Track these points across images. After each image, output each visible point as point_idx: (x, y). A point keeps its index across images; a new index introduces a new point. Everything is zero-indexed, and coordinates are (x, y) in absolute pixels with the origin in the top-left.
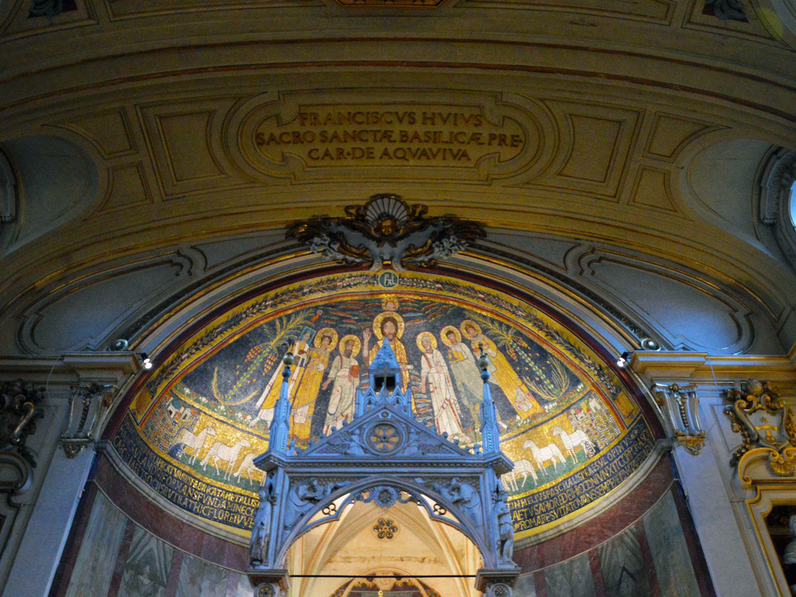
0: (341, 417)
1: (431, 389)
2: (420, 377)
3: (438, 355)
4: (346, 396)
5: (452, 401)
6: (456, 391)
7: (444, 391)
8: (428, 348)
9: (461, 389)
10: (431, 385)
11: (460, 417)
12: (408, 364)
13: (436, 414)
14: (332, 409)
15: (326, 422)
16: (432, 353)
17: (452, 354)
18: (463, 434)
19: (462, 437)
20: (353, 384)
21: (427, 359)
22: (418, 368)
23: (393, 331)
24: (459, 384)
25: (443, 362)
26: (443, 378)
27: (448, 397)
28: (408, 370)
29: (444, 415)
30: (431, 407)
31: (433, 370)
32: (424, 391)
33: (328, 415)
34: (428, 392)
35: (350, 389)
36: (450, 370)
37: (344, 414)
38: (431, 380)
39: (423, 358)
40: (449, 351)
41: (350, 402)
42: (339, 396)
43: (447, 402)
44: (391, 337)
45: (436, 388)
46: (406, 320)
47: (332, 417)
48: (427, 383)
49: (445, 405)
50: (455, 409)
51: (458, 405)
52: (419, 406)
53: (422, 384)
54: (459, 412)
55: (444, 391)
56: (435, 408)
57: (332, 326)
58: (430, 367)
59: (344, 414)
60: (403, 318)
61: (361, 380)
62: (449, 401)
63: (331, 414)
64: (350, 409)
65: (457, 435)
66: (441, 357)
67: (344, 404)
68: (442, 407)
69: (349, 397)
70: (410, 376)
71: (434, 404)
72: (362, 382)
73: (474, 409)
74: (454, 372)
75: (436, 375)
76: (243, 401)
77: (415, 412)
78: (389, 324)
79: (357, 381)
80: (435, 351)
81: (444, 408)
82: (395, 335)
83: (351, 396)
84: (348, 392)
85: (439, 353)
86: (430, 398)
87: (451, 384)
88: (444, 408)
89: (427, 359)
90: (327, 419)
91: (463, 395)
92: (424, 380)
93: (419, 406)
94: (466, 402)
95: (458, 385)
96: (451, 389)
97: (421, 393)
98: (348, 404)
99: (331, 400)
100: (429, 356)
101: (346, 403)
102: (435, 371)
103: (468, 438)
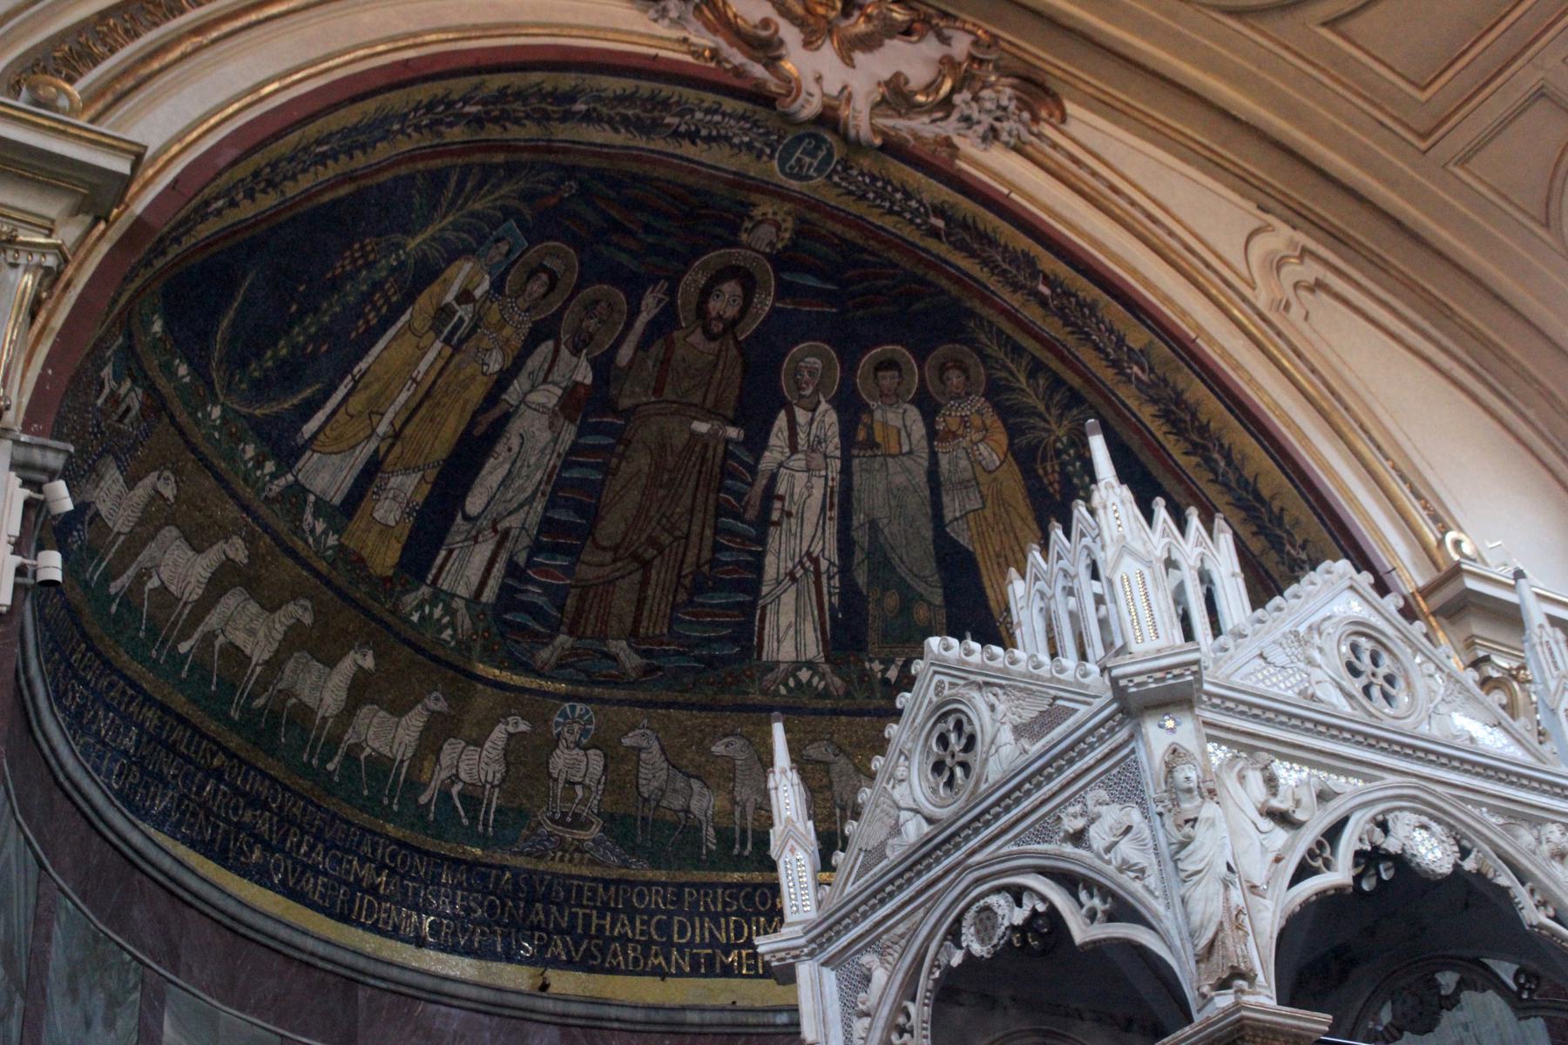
0: (488, 533)
1: (775, 516)
2: (753, 470)
3: (829, 418)
4: (524, 472)
5: (824, 565)
6: (846, 544)
7: (808, 530)
8: (808, 392)
9: (861, 536)
10: (777, 505)
11: (833, 618)
12: (734, 423)
13: (765, 590)
14: (475, 503)
15: (449, 540)
16: (814, 410)
17: (870, 428)
18: (827, 668)
19: (823, 677)
20: (555, 441)
21: (792, 424)
22: (757, 442)
24: (859, 519)
25: (833, 445)
26: (818, 493)
27: (816, 551)
28: (728, 441)
29: (789, 598)
30: (759, 568)
31: (798, 461)
32: (751, 514)
33: (459, 517)
34: (764, 522)
35: (543, 451)
36: (846, 471)
37: (501, 526)
38: (782, 489)
39: (782, 415)
40: (865, 418)
41: (527, 494)
42: (507, 466)
43: (808, 564)
45: (789, 515)
47: (467, 526)
48: (770, 495)
49: (799, 573)
50: (825, 590)
51: (836, 582)
52: (725, 557)
54: (835, 600)
55: (808, 530)
56: (770, 572)
58: (794, 448)
59: (501, 526)
61: (579, 435)
62: (815, 561)
63: (466, 518)
64: (522, 514)
65: (810, 665)
66: (836, 429)
67: (510, 495)
68: (792, 576)
69: (533, 478)
70: (725, 459)
71: (770, 560)
72: (582, 441)
73: (879, 602)
74: (856, 480)
75: (801, 478)
77: (706, 569)
79: (569, 434)
80: (824, 406)
81: (794, 579)
83: (538, 476)
84: (533, 460)
85: (832, 417)
86: (762, 540)
87: (835, 513)
88: (794, 579)
89: (792, 424)
90: (454, 529)
91: (859, 556)
92: (762, 482)
93: (725, 557)
94: (861, 579)
95: (855, 523)
96: (832, 529)
97: (738, 517)
98: (522, 497)
99: (484, 472)
100: (802, 416)
101: (514, 496)
102: (803, 464)
103: (838, 681)
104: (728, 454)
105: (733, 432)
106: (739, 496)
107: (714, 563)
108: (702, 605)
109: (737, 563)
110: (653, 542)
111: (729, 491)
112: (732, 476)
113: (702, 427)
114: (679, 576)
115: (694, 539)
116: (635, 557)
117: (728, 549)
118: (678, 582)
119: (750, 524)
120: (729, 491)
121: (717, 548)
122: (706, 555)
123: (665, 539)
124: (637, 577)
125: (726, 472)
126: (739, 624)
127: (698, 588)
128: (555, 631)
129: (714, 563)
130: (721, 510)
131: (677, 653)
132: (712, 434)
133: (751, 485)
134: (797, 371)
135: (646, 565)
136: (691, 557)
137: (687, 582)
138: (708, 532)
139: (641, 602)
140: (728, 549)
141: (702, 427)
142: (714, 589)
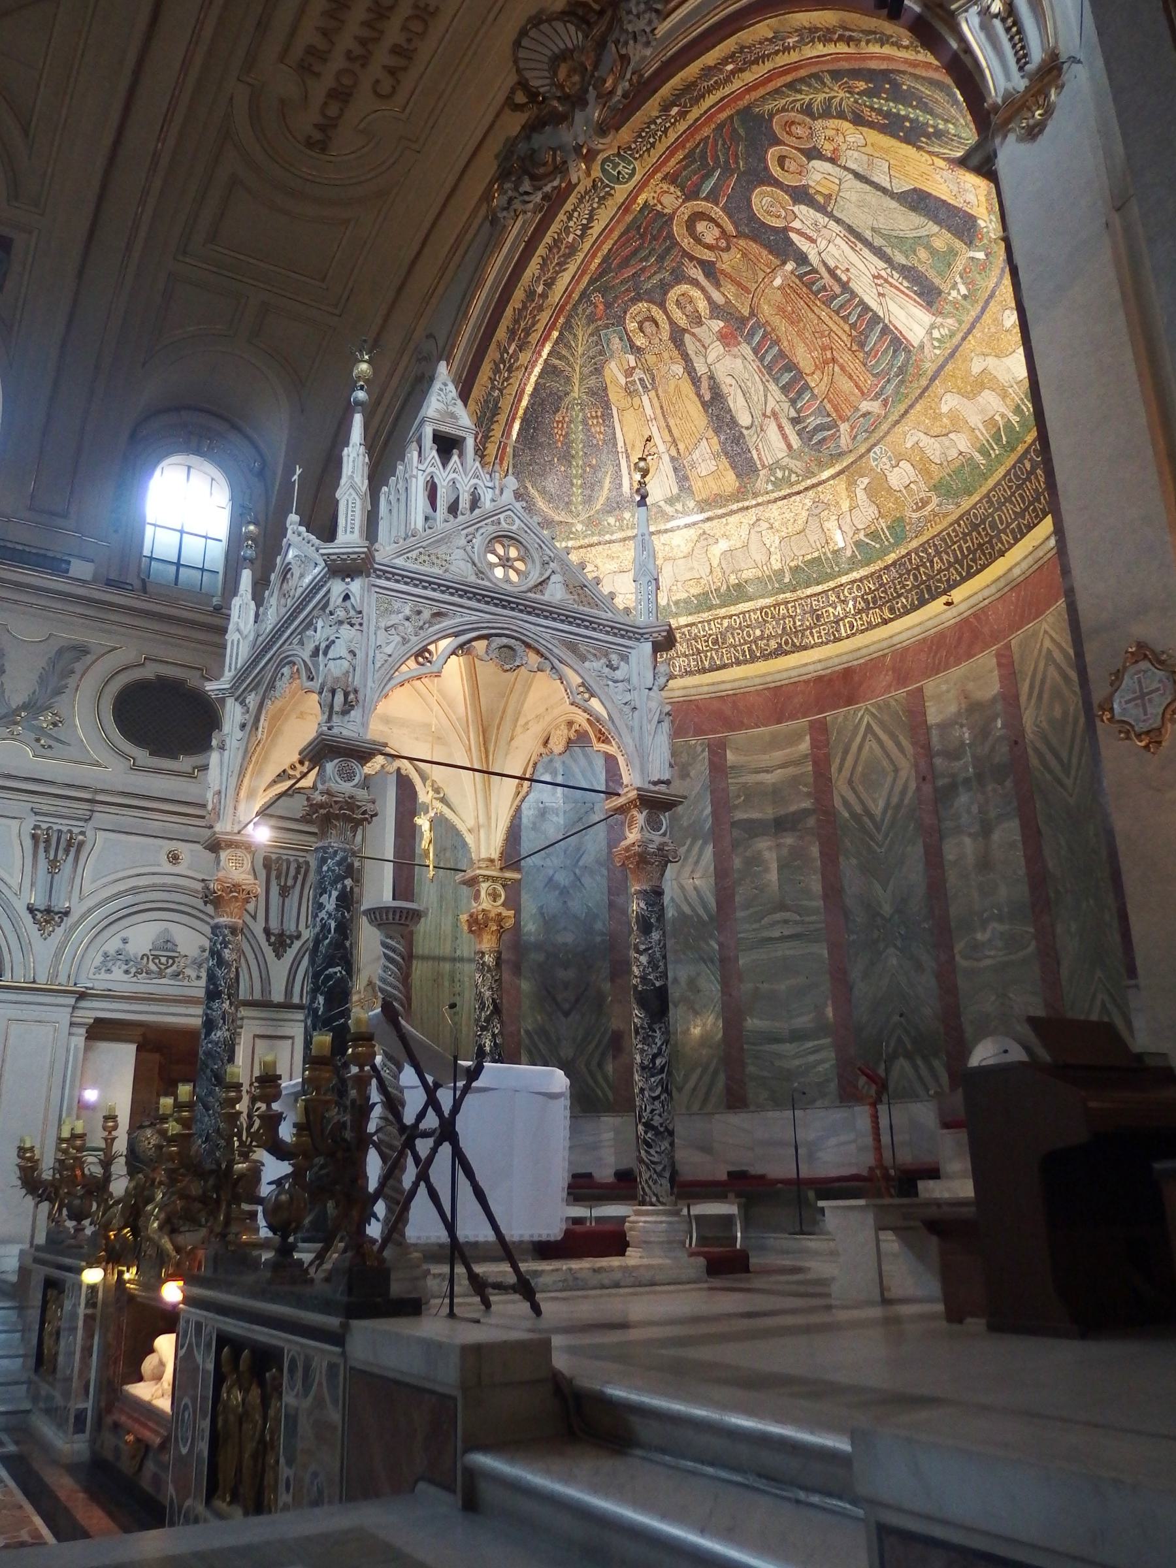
12: (784, 263)
22: (802, 259)
23: (716, 232)
28: (792, 272)
39: (793, 236)
44: (723, 244)
46: (713, 197)
52: (852, 319)
53: (827, 279)
57: (634, 301)
60: (706, 199)
76: (602, 500)
77: (854, 333)
78: (701, 227)
82: (723, 232)
93: (852, 319)
97: (837, 296)
104: (800, 277)
105: (790, 266)
106: (824, 288)
107: (853, 326)
108: (871, 349)
109: (859, 316)
110: (824, 348)
111: (819, 291)
112: (813, 283)
113: (778, 282)
114: (850, 349)
115: (835, 328)
116: (826, 362)
117: (850, 314)
118: (853, 352)
119: (842, 293)
120: (819, 291)
121: (845, 319)
122: (847, 328)
123: (826, 341)
124: (837, 368)
125: (808, 286)
126: (891, 341)
127: (862, 345)
128: (834, 425)
129: (853, 326)
130: (827, 302)
131: (888, 381)
132: (785, 278)
133: (822, 278)
134: (768, 213)
135: (834, 360)
136: (840, 333)
137: (855, 348)
138: (836, 318)
139: (850, 377)
140: (850, 314)
141: (778, 282)
142: (867, 337)
